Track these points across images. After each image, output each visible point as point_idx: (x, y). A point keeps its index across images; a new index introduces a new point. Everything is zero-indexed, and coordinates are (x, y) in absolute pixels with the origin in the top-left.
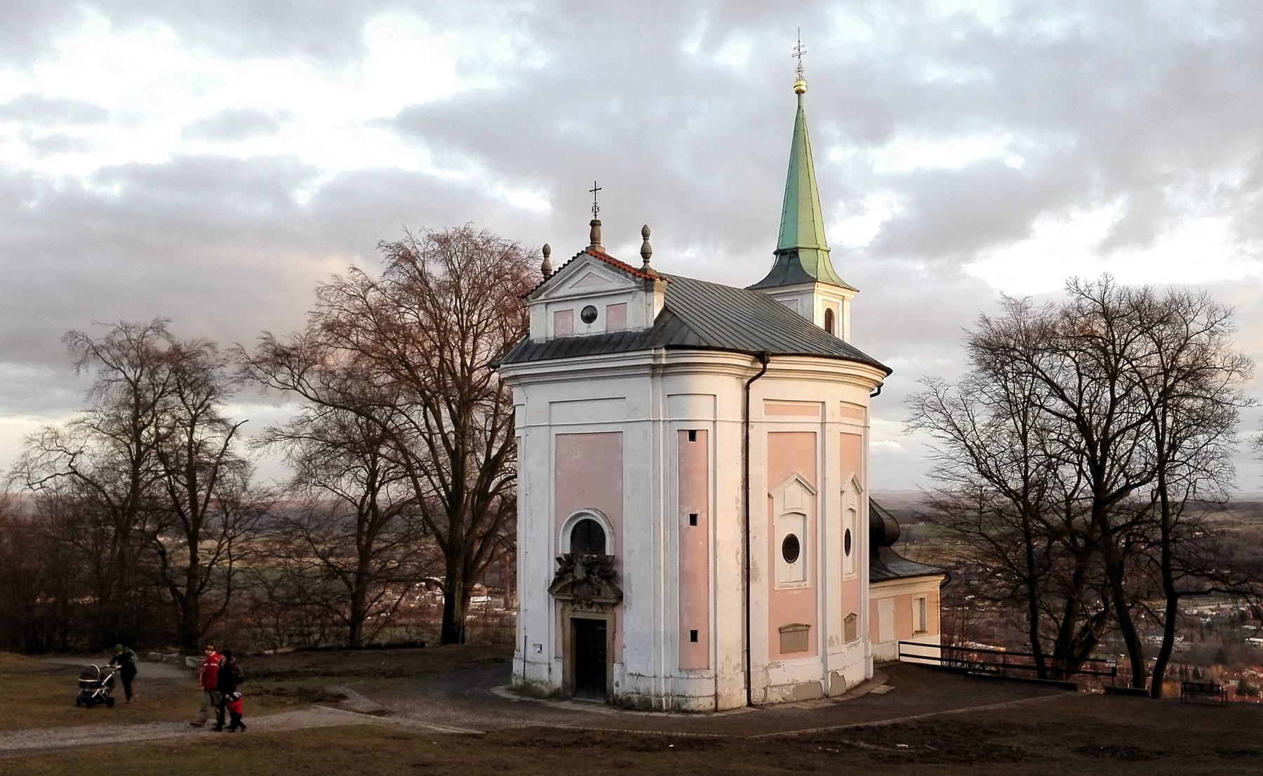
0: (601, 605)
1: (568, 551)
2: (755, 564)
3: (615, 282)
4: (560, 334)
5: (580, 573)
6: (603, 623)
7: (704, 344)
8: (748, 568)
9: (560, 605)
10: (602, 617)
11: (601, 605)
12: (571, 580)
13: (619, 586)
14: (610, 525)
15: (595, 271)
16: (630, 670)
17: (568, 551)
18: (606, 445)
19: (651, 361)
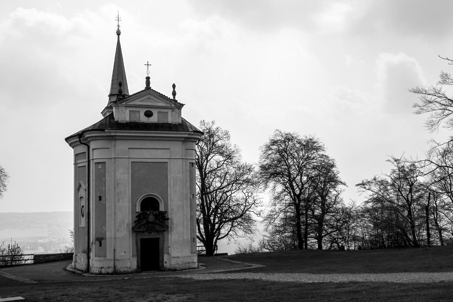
0: (158, 232)
5: (151, 218)
6: (158, 239)
9: (135, 234)
10: (158, 236)
12: (144, 222)
17: (139, 211)
18: (161, 167)
19: (187, 136)
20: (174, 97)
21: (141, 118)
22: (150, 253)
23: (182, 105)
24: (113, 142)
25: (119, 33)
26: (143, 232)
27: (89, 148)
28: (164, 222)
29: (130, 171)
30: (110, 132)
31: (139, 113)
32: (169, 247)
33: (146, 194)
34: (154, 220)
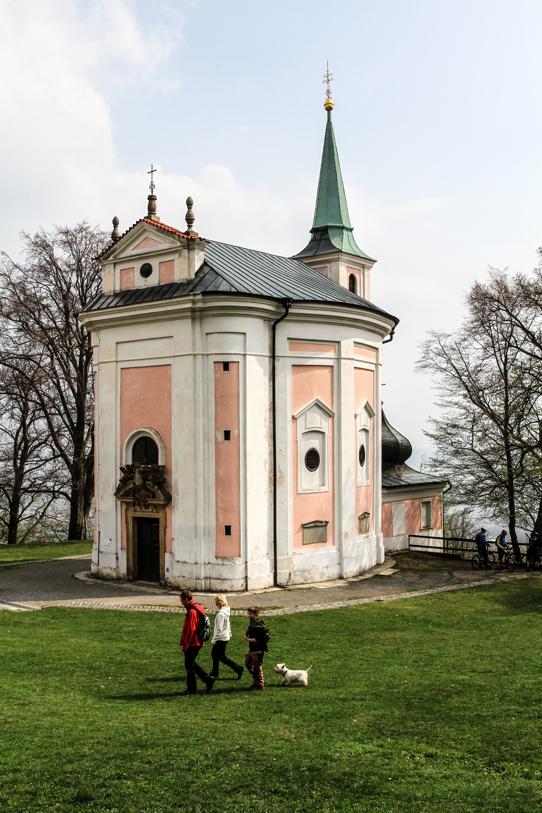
1: (130, 463)
2: (280, 472)
3: (164, 244)
4: (124, 288)
5: (138, 479)
6: (157, 520)
7: (233, 290)
8: (275, 475)
11: (155, 506)
12: (132, 486)
13: (167, 490)
14: (161, 440)
15: (151, 236)
16: (177, 558)
17: (130, 463)
19: (190, 305)
20: (189, 227)
25: (329, 109)
31: (134, 272)
32: (173, 540)
33: (136, 431)
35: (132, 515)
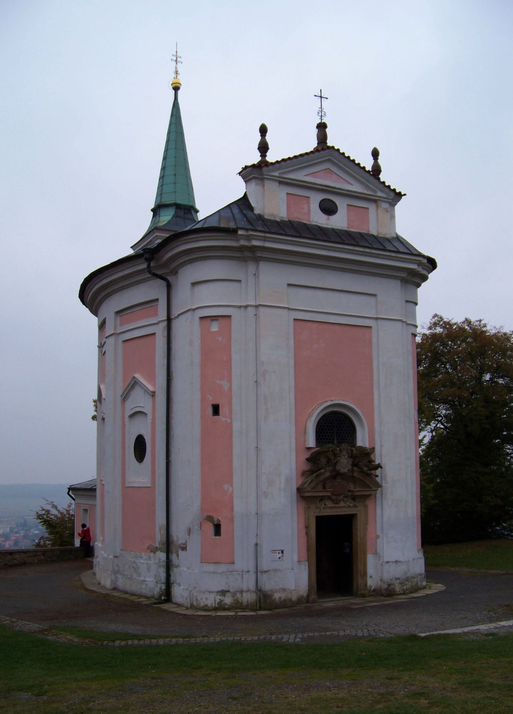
5: (344, 464)
21: (312, 214)
22: (335, 549)
23: (399, 196)
24: (251, 267)
25: (176, 89)
26: (322, 499)
27: (169, 286)
28: (370, 475)
29: (292, 342)
30: (249, 238)
31: (309, 203)
32: (378, 537)
34: (350, 467)
35: (316, 514)
